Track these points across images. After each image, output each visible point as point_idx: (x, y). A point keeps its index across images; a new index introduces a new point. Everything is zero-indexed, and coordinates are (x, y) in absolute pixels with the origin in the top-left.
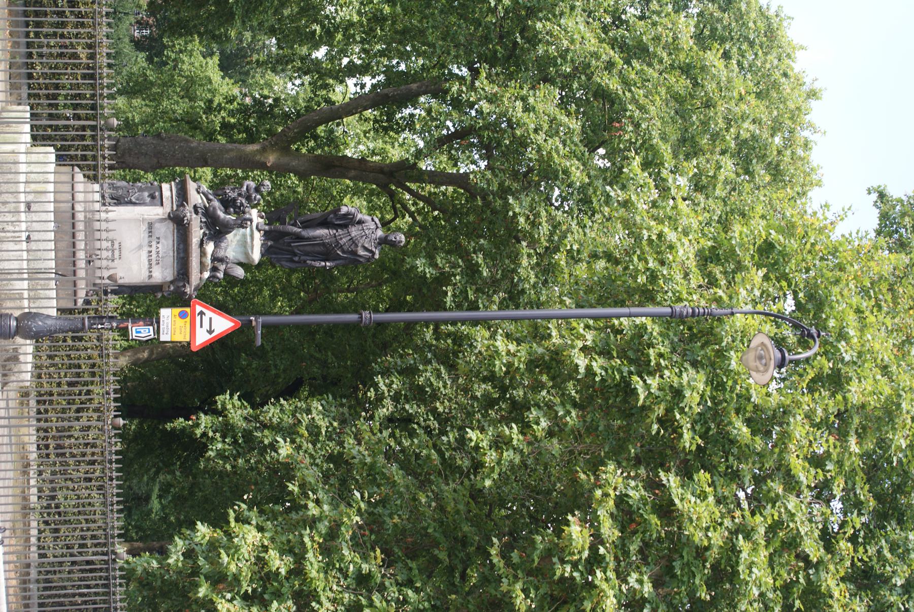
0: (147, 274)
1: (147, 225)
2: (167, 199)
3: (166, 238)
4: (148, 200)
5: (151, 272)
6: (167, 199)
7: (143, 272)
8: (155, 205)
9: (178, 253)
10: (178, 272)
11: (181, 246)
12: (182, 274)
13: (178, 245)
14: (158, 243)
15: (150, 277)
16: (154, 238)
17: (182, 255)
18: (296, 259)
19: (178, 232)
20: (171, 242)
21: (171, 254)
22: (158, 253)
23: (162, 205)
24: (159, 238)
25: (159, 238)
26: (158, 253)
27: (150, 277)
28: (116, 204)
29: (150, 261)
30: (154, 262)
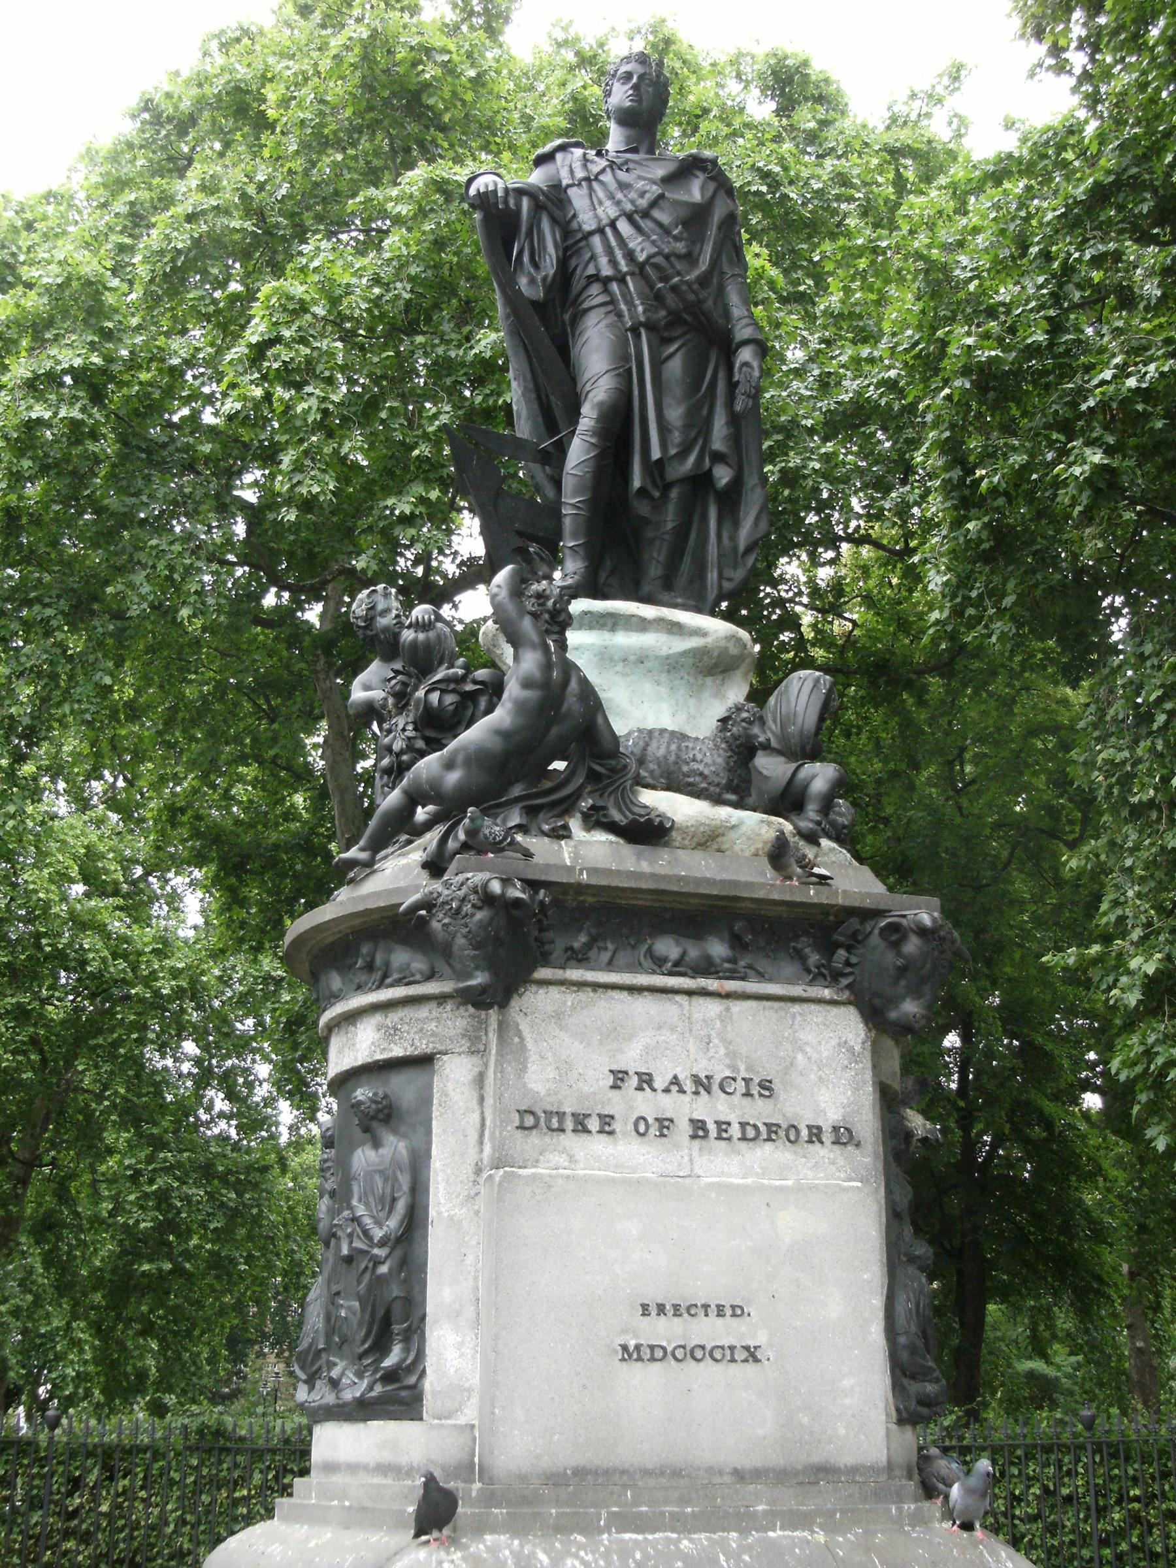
0: (824, 1152)
1: (535, 1140)
2: (392, 1033)
3: (616, 1034)
4: (395, 1146)
5: (816, 1134)
6: (392, 1033)
7: (818, 1179)
8: (426, 1101)
9: (706, 968)
10: (818, 976)
11: (668, 947)
12: (829, 948)
13: (658, 963)
14: (646, 1080)
15: (844, 1136)
16: (615, 1104)
17: (718, 949)
18: (723, 475)
19: (579, 958)
20: (645, 1006)
21: (712, 1007)
22: (702, 1084)
23: (424, 1062)
24: (619, 1077)
25: (619, 1077)
26: (702, 1084)
27: (844, 1136)
28: (415, 1333)
29: (751, 1134)
30: (759, 1111)
